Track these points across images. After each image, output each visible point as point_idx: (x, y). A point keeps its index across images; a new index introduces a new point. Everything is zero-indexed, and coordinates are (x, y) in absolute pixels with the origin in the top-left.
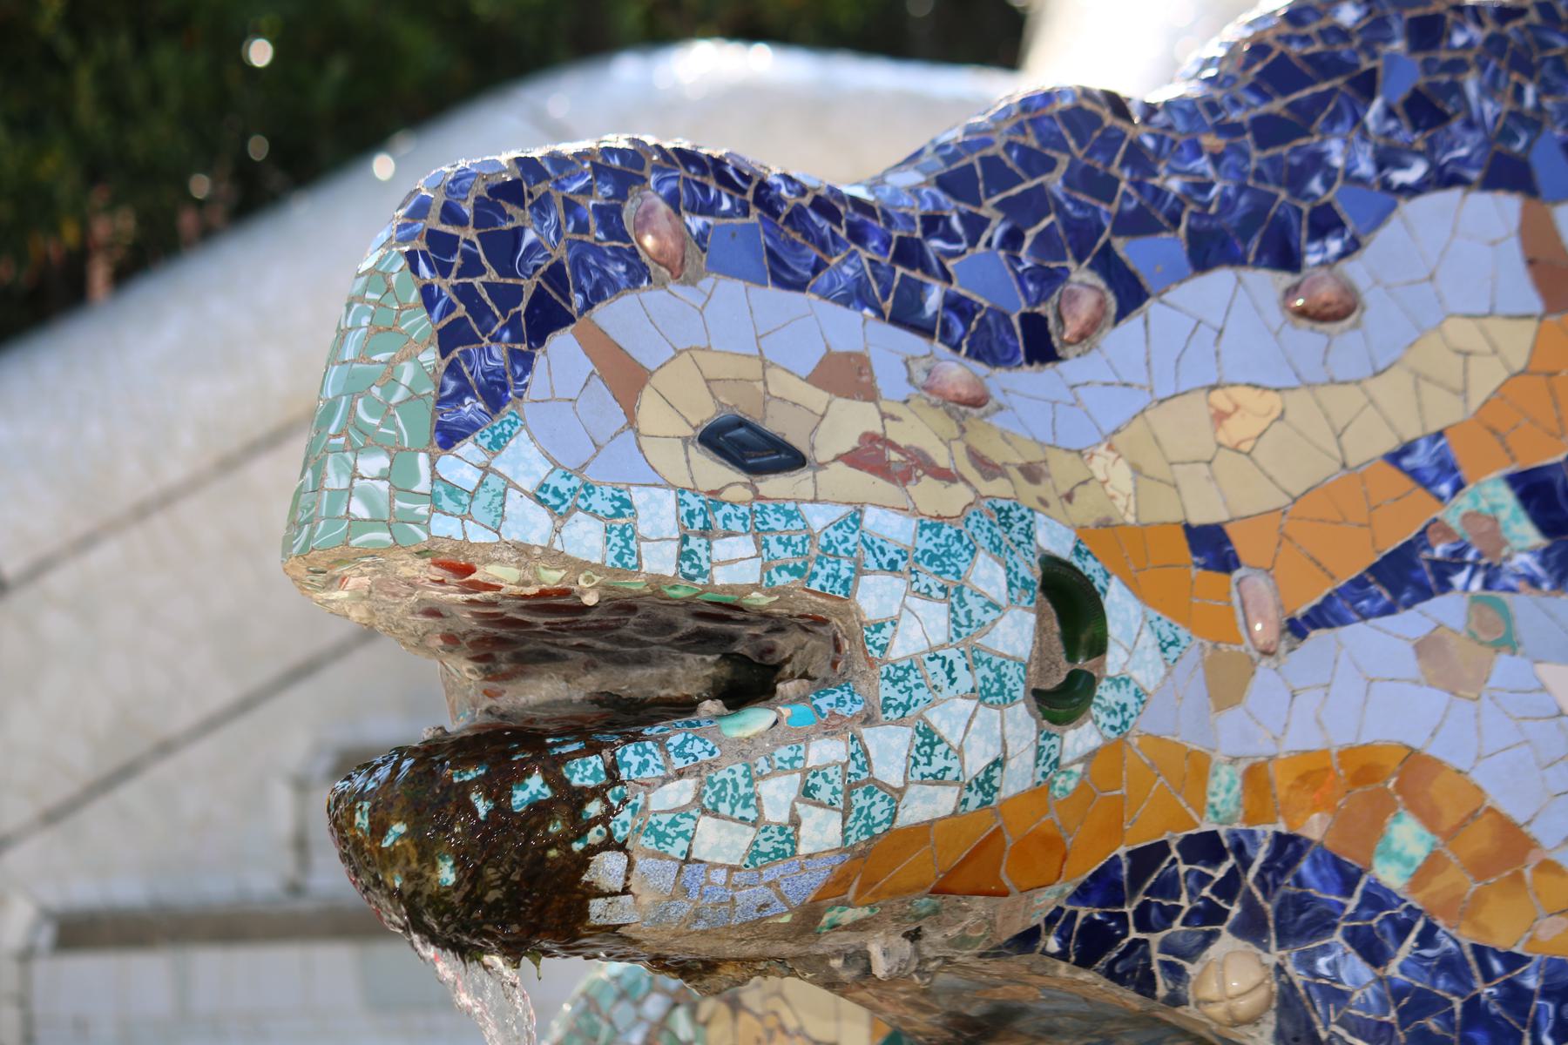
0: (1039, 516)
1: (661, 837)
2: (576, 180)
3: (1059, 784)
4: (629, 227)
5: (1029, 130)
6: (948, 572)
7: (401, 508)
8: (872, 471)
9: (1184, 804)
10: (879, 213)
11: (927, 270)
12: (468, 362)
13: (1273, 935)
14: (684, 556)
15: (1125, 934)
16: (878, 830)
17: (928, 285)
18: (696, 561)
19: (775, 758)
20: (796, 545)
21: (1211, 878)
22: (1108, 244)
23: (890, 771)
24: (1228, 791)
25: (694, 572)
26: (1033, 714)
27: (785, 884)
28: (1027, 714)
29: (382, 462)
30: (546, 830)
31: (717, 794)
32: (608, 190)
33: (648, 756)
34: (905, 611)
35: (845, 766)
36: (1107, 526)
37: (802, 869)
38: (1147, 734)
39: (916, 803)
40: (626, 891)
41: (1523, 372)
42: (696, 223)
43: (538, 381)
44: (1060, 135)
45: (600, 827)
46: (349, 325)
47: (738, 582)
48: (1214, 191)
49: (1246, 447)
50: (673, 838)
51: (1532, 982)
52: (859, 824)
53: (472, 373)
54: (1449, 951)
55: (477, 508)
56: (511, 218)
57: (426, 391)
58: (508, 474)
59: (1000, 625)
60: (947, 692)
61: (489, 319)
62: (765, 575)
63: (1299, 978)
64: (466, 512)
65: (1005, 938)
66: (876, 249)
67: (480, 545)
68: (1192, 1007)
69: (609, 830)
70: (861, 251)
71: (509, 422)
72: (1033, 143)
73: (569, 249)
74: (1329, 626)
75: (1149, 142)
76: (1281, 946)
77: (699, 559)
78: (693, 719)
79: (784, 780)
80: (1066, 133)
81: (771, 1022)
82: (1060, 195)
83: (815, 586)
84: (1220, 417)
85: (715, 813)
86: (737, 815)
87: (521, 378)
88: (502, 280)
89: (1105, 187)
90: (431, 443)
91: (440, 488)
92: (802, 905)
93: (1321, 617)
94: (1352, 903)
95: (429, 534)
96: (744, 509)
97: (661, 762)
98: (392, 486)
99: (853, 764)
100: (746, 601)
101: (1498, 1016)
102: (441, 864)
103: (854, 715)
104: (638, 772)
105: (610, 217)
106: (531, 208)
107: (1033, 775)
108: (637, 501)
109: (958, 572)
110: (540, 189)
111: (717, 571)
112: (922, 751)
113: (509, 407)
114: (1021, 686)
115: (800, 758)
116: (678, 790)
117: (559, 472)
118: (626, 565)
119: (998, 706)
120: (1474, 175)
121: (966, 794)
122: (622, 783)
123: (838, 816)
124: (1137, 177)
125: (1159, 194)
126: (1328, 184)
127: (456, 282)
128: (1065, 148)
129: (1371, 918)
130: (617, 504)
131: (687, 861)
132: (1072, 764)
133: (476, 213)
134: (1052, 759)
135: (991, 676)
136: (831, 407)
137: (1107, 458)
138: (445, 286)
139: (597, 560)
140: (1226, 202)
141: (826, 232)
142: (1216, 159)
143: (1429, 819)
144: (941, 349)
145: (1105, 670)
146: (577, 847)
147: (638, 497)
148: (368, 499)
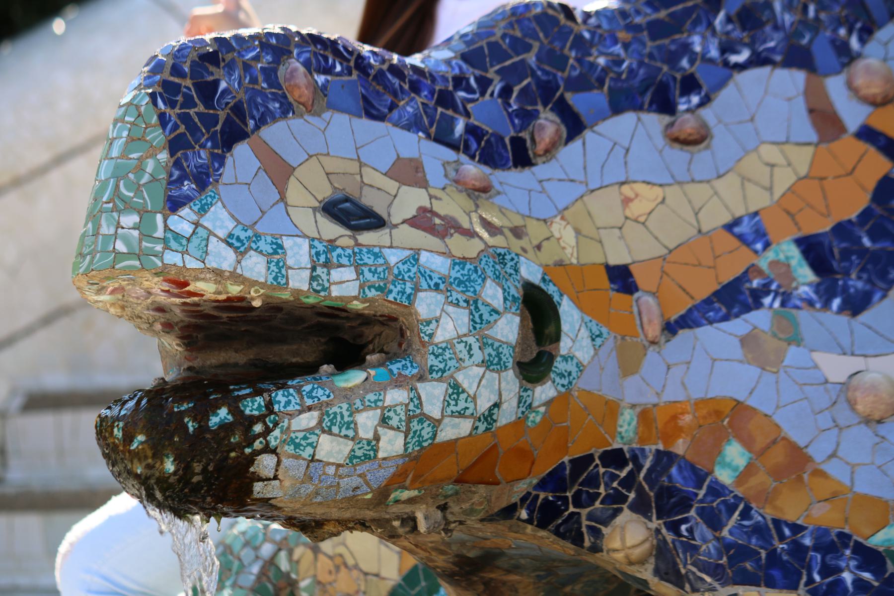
0: (522, 259)
1: (297, 446)
2: (251, 51)
3: (531, 418)
4: (281, 80)
5: (516, 26)
6: (469, 291)
7: (146, 247)
8: (425, 229)
9: (603, 432)
10: (427, 75)
11: (456, 110)
13: (654, 511)
14: (313, 278)
15: (567, 509)
16: (425, 444)
17: (457, 119)
18: (321, 282)
19: (366, 400)
20: (380, 273)
21: (619, 476)
22: (562, 96)
23: (433, 409)
24: (629, 424)
25: (319, 288)
26: (517, 377)
27: (369, 475)
28: (514, 376)
29: (134, 219)
30: (229, 440)
32: (269, 58)
33: (290, 398)
34: (443, 314)
35: (407, 405)
36: (561, 265)
37: (380, 466)
38: (583, 390)
39: (448, 428)
40: (275, 478)
41: (805, 177)
42: (321, 79)
43: (228, 172)
44: (534, 30)
45: (261, 439)
46: (115, 136)
47: (345, 295)
48: (625, 65)
49: (642, 219)
50: (305, 447)
51: (808, 542)
52: (414, 440)
53: (188, 166)
54: (759, 522)
55: (192, 247)
56: (212, 74)
57: (161, 177)
58: (210, 228)
59: (499, 323)
60: (467, 363)
61: (199, 134)
62: (362, 291)
64: (185, 250)
65: (496, 510)
66: (426, 96)
67: (193, 269)
68: (605, 553)
69: (267, 441)
70: (417, 98)
71: (210, 196)
72: (518, 34)
73: (246, 93)
74: (690, 327)
75: (587, 35)
76: (658, 518)
77: (323, 280)
78: (317, 376)
79: (371, 413)
80: (538, 29)
81: (338, 561)
82: (534, 66)
83: (391, 298)
84: (627, 201)
85: (330, 432)
86: (342, 434)
87: (218, 170)
88: (206, 111)
89: (561, 62)
90: (164, 208)
91: (169, 235)
92: (379, 488)
93: (686, 322)
94: (702, 493)
95: (162, 262)
96: (349, 251)
97: (298, 401)
98: (141, 234)
99: (412, 404)
100: (349, 306)
101: (787, 561)
102: (166, 460)
103: (413, 375)
104: (285, 407)
105: (270, 74)
106: (224, 68)
107: (517, 413)
109: (475, 291)
110: (229, 57)
111: (333, 288)
112: (452, 397)
113: (210, 187)
114: (511, 360)
115: (381, 400)
116: (308, 418)
117: (240, 227)
118: (279, 283)
119: (498, 372)
120: (778, 58)
121: (477, 424)
122: (275, 413)
123: (402, 435)
124: (579, 55)
125: (593, 66)
126: (692, 62)
127: (179, 111)
128: (537, 38)
129: (713, 502)
130: (274, 247)
131: (312, 460)
132: (539, 406)
134: (527, 404)
135: (494, 353)
136: (400, 191)
137: (560, 224)
138: (173, 114)
139: (262, 280)
140: (631, 71)
141: (397, 85)
142: (626, 46)
143: (747, 443)
144: (463, 158)
145: (559, 351)
146: (248, 451)
147: (287, 242)
148: (126, 241)
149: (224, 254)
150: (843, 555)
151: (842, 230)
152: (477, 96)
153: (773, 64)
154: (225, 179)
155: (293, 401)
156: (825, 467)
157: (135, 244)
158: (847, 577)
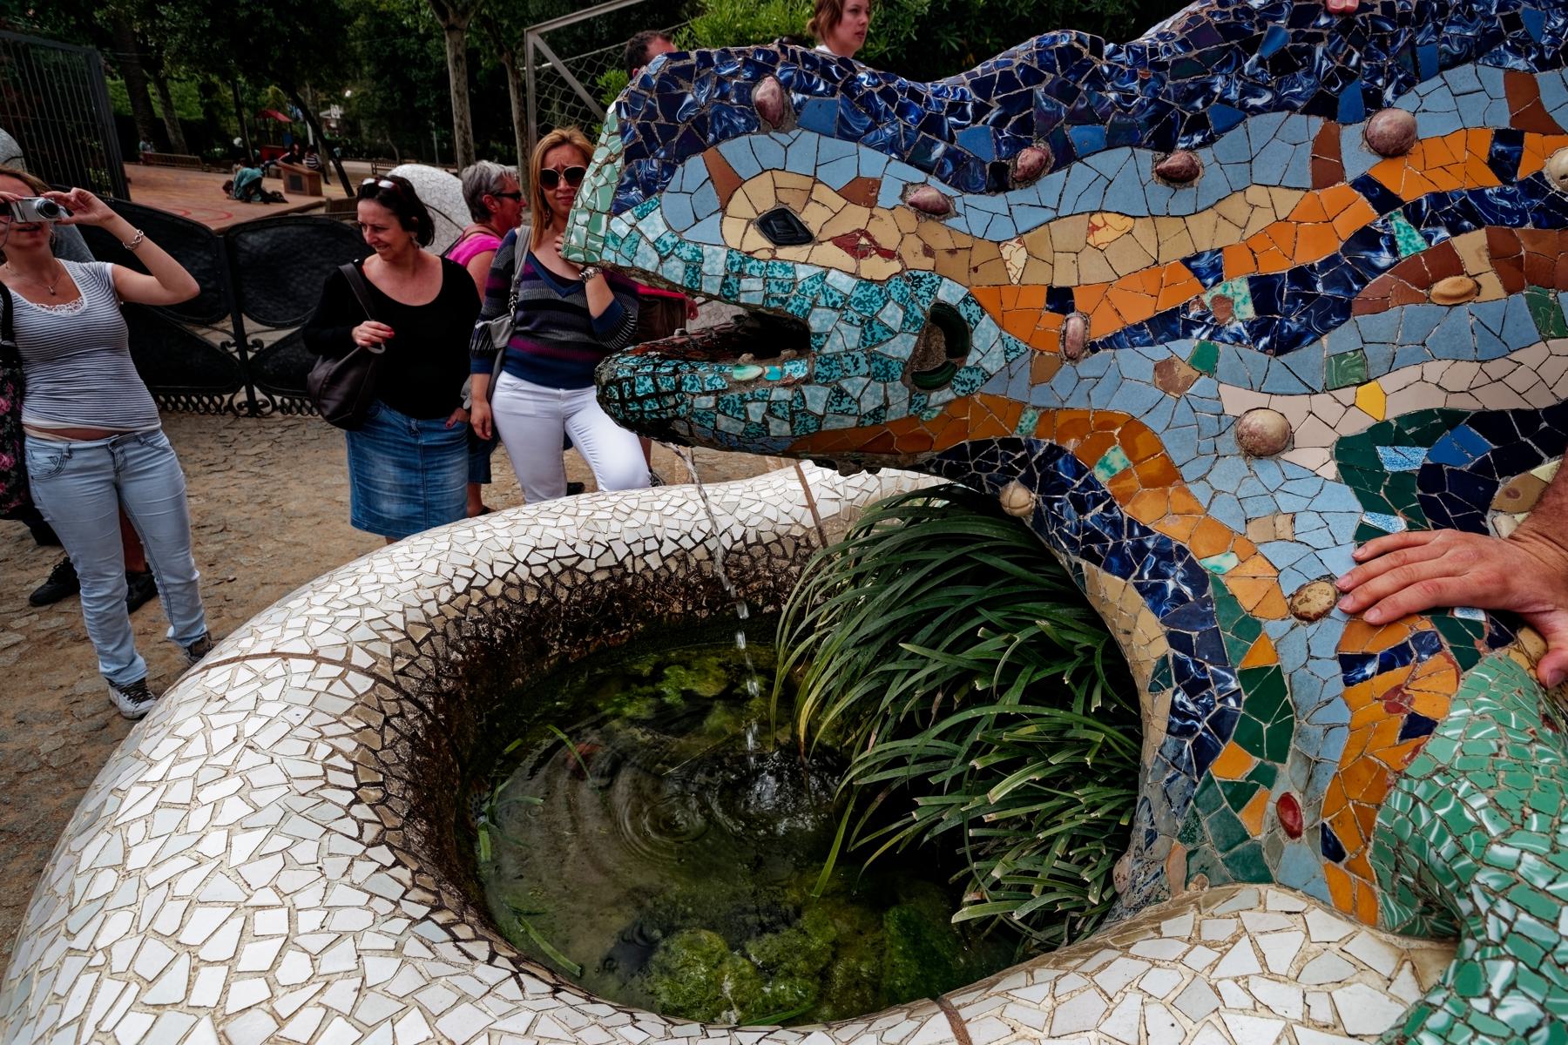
14: (724, 285)
35: (790, 402)
42: (797, 98)
43: (674, 183)
49: (1102, 247)
51: (1150, 545)
60: (852, 374)
70: (901, 121)
72: (1035, 66)
75: (1106, 70)
79: (759, 404)
84: (1094, 229)
85: (724, 413)
93: (1112, 342)
94: (1078, 483)
105: (745, 91)
108: (705, 254)
111: (742, 295)
113: (656, 195)
120: (1300, 104)
125: (1102, 100)
126: (1205, 104)
128: (1054, 72)
135: (881, 367)
139: (679, 282)
140: (1140, 106)
141: (883, 108)
142: (1143, 83)
143: (1130, 452)
147: (707, 250)
149: (649, 255)
153: (1293, 109)
156: (1189, 486)
157: (583, 239)
158: (1171, 585)
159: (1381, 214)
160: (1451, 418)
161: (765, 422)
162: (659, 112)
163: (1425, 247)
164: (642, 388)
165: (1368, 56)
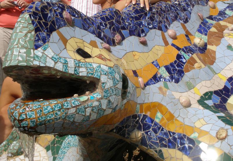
1: (69, 118)
12: (40, 34)
14: (75, 70)
16: (101, 116)
23: (104, 107)
25: (77, 73)
29: (25, 50)
31: (79, 111)
32: (60, 10)
33: (68, 104)
35: (98, 106)
42: (73, 18)
43: (51, 39)
49: (137, 60)
51: (176, 137)
52: (99, 115)
55: (42, 60)
56: (46, 12)
58: (47, 54)
61: (43, 28)
63: (145, 135)
75: (124, 17)
76: (143, 131)
79: (89, 108)
83: (95, 77)
84: (134, 55)
85: (78, 113)
87: (48, 38)
91: (35, 56)
94: (153, 124)
98: (26, 55)
100: (84, 79)
104: (67, 107)
105: (61, 14)
106: (49, 10)
113: (47, 43)
117: (55, 55)
125: (125, 24)
126: (143, 26)
128: (115, 17)
129: (155, 127)
130: (65, 61)
133: (41, 10)
135: (118, 92)
138: (36, 22)
139: (61, 70)
142: (131, 21)
143: (162, 112)
144: (104, 42)
147: (68, 60)
148: (22, 57)
150: (185, 140)
151: (172, 65)
152: (105, 28)
153: (156, 29)
154: (50, 41)
155: (69, 105)
156: (177, 119)
158: (187, 145)
159: (179, 51)
160: (211, 92)
161: (90, 114)
162: (42, 18)
163: (189, 58)
164: (47, 111)
165: (162, 19)
